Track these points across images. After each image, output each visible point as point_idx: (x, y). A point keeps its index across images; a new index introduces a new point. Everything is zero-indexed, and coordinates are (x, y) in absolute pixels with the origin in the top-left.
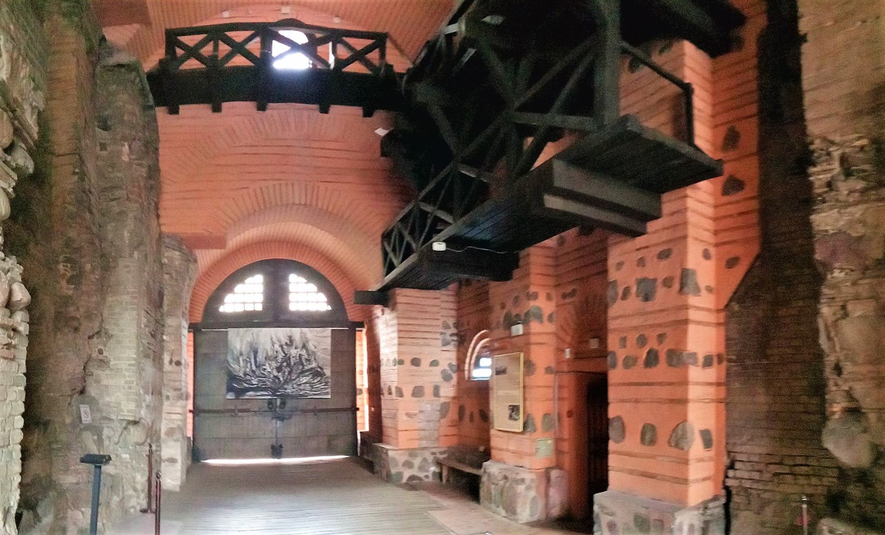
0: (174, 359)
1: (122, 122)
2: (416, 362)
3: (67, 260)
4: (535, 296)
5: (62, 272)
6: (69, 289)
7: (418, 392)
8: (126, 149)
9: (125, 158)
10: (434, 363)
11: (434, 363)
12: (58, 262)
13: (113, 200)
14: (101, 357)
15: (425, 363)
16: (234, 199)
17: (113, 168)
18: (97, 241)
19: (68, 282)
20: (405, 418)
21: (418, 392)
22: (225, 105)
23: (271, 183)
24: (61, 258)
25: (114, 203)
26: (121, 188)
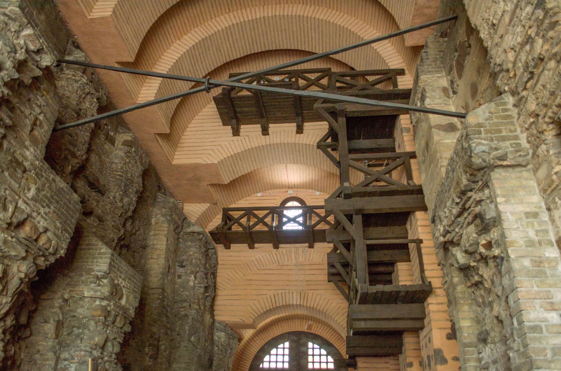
1: (191, 263)
5: (147, 352)
6: (149, 361)
9: (191, 284)
12: (145, 347)
13: (182, 308)
17: (184, 289)
18: (169, 332)
19: (150, 358)
23: (280, 292)
24: (147, 344)
25: (182, 309)
26: (185, 301)
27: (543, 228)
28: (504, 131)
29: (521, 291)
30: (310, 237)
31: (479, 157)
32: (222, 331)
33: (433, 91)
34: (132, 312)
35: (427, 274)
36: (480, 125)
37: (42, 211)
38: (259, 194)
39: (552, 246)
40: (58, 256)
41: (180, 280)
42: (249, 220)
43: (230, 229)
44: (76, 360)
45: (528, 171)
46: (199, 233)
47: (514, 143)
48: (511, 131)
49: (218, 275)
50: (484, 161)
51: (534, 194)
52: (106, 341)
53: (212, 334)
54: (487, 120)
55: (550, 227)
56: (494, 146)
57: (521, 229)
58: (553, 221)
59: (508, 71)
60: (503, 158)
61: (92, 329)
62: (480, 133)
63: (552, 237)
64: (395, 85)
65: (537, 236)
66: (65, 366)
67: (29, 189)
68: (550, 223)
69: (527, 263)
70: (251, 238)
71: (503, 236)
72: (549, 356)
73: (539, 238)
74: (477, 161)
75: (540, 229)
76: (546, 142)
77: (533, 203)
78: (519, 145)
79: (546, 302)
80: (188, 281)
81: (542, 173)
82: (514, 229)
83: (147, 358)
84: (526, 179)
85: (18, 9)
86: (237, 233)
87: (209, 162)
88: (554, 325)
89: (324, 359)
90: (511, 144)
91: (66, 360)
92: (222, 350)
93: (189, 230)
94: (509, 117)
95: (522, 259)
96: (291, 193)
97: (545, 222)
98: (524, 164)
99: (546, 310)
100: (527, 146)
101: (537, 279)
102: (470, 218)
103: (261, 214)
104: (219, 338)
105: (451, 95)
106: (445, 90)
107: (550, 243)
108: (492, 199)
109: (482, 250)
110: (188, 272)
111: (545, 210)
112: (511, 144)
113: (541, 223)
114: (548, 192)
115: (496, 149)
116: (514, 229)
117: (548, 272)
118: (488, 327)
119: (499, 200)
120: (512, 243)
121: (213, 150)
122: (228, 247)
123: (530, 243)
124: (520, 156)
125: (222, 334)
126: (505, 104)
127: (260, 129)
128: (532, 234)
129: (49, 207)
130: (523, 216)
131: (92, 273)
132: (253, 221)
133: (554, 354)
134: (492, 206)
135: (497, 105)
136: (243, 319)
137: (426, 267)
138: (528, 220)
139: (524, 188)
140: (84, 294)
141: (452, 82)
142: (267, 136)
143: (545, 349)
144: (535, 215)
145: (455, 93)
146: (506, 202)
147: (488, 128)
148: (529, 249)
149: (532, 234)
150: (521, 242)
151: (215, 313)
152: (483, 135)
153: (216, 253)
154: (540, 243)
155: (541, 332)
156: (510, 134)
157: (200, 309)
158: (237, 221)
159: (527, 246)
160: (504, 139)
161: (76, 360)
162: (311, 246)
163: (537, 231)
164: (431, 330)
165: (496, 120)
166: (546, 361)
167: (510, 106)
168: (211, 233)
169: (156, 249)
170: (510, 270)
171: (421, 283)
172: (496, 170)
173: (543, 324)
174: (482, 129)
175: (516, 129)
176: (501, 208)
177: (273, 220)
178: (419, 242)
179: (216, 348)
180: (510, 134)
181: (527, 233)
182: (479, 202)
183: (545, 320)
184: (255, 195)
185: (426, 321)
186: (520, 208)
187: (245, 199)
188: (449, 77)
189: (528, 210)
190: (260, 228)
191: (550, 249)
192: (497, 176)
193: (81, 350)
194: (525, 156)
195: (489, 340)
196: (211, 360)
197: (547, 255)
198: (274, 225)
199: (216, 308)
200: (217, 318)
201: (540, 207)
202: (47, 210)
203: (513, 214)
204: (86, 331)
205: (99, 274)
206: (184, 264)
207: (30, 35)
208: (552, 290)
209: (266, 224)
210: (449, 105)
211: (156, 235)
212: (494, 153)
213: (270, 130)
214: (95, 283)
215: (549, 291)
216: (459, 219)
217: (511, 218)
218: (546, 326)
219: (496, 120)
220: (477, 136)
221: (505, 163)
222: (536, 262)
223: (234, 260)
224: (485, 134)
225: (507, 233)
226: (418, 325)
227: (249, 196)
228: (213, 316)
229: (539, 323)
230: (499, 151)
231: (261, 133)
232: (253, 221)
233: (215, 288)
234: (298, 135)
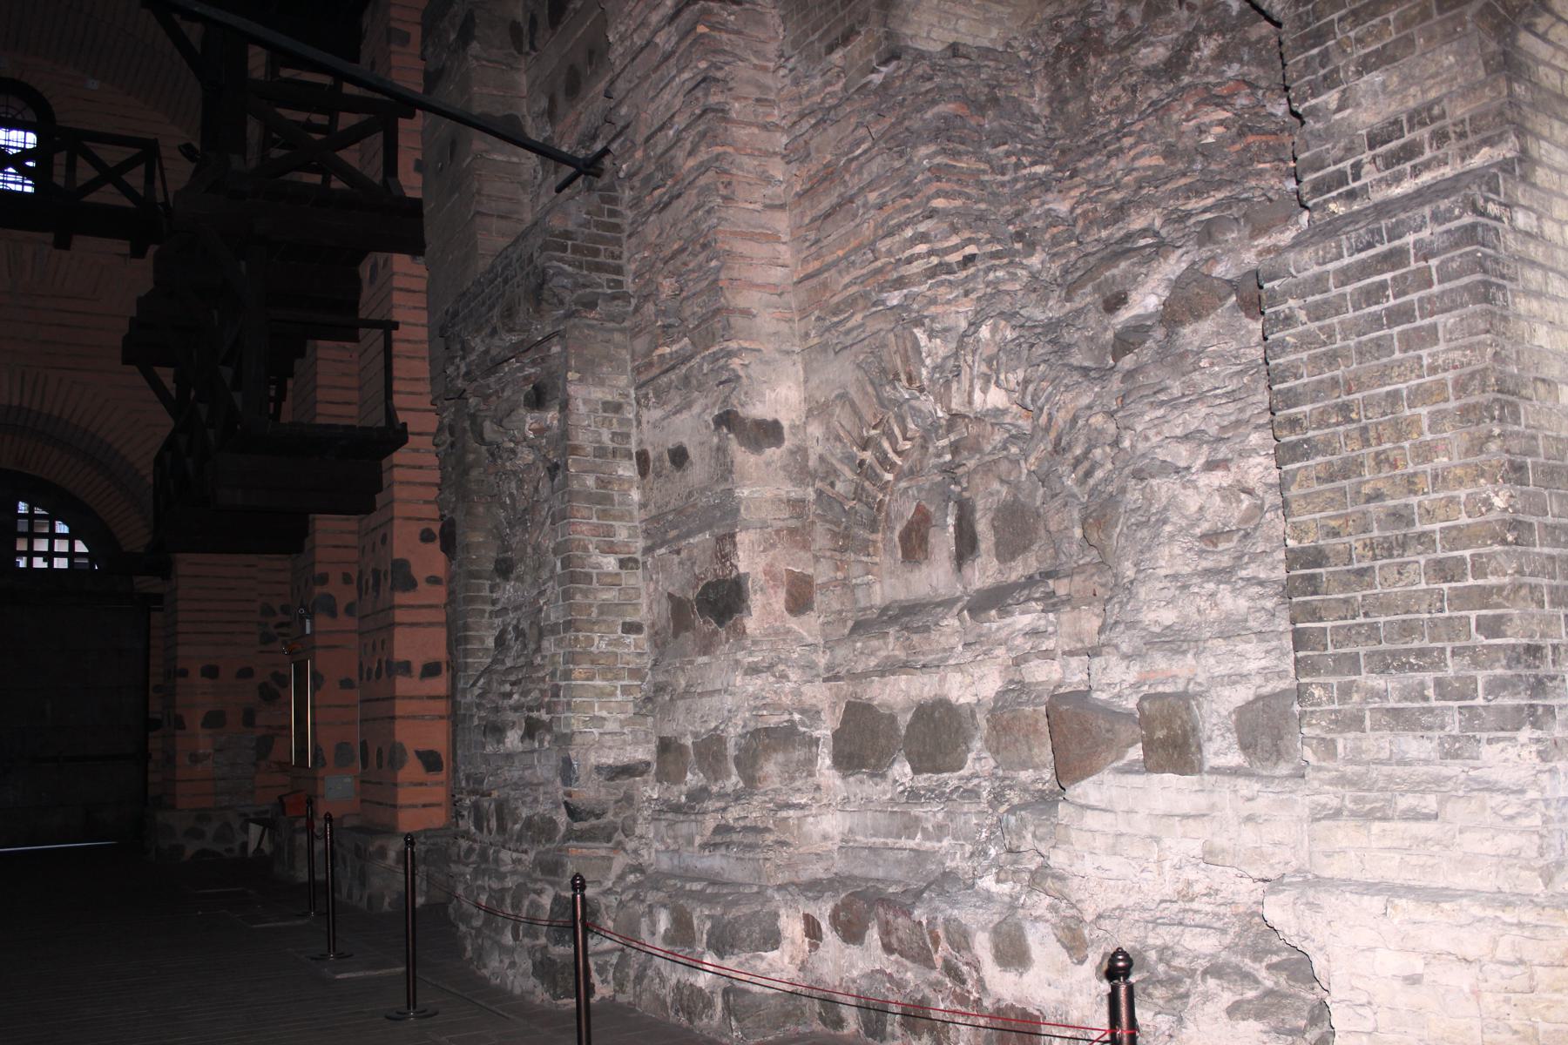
2: (211, 672)
4: (324, 579)
7: (214, 720)
10: (246, 673)
11: (246, 673)
27: (625, 430)
35: (398, 400)
36: (567, 235)
51: (624, 372)
56: (581, 280)
69: (590, 481)
78: (619, 284)
84: (617, 346)
88: (609, 574)
89: (61, 546)
90: (609, 281)
95: (585, 476)
105: (527, 48)
113: (624, 422)
115: (584, 286)
117: (616, 498)
123: (601, 452)
133: (601, 613)
137: (397, 386)
139: (610, 359)
143: (591, 605)
144: (617, 408)
146: (580, 380)
150: (589, 449)
152: (569, 255)
154: (614, 453)
160: (599, 268)
163: (614, 434)
164: (392, 519)
166: (589, 621)
171: (382, 424)
176: (571, 389)
183: (599, 566)
185: (380, 499)
186: (598, 394)
189: (609, 398)
191: (626, 463)
201: (627, 396)
203: (585, 402)
208: (616, 524)
217: (582, 409)
219: (594, 230)
224: (574, 252)
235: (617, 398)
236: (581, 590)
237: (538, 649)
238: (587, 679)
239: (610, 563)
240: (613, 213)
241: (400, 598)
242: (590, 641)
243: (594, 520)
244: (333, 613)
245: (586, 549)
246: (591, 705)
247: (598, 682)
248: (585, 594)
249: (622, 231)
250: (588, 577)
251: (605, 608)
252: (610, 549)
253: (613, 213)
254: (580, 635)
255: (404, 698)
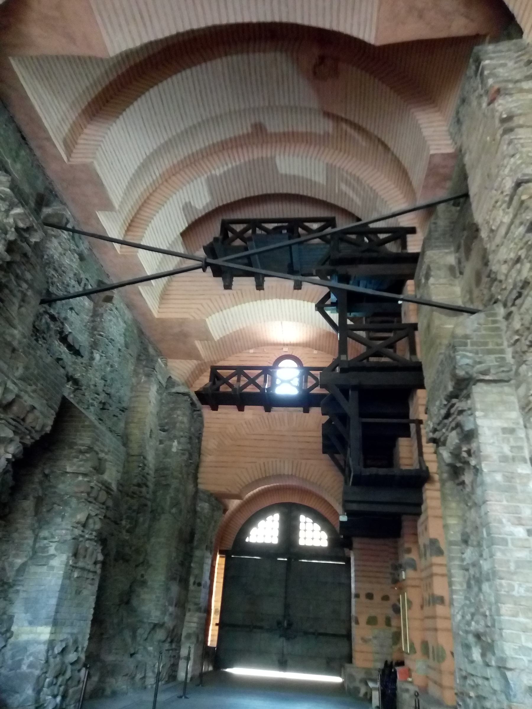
0: (197, 581)
2: (370, 596)
3: (128, 518)
8: (175, 443)
9: (174, 450)
10: (386, 598)
14: (142, 579)
15: (377, 598)
16: (247, 469)
20: (360, 642)
21: (372, 621)
22: (246, 407)
27: (519, 444)
28: (490, 343)
29: (490, 505)
30: (306, 401)
31: (463, 370)
32: (206, 502)
33: (439, 269)
34: (114, 486)
35: (426, 457)
36: (466, 337)
37: (29, 389)
38: (251, 351)
39: (526, 462)
40: (43, 433)
41: (162, 446)
42: (239, 380)
43: (218, 389)
44: (56, 539)
45: (510, 386)
46: (184, 394)
47: (500, 358)
48: (498, 345)
49: (203, 438)
50: (467, 373)
51: (514, 410)
52: (88, 518)
53: (194, 505)
54: (475, 331)
55: (525, 445)
56: (478, 360)
57: (497, 444)
58: (528, 438)
59: (501, 281)
60: (485, 372)
61: (73, 506)
62: (466, 345)
63: (527, 454)
64: (404, 245)
65: (511, 452)
66: (44, 545)
67: (17, 368)
68: (525, 440)
69: (499, 477)
70: (240, 400)
71: (479, 449)
72: (512, 567)
73: (514, 454)
74: (461, 373)
75: (515, 445)
76: (527, 363)
77: (511, 419)
78: (503, 359)
79: (515, 517)
80: (171, 446)
81: (522, 390)
82: (490, 444)
83: (124, 532)
84: (508, 394)
85: (8, 190)
86: (225, 394)
87: (197, 318)
88: (520, 539)
90: (496, 358)
91: (45, 538)
92: (204, 523)
93: (174, 390)
94: (498, 329)
96: (286, 351)
97: (521, 438)
98: (506, 379)
99: (513, 524)
100: (512, 361)
101: (506, 494)
102: (453, 424)
103: (252, 373)
104: (203, 508)
105: (458, 274)
106: (451, 269)
107: (524, 460)
108: (471, 411)
109: (464, 455)
110: (172, 436)
111: (522, 427)
112: (496, 358)
114: (527, 410)
115: (480, 363)
116: (490, 444)
117: (519, 488)
118: (468, 530)
119: (477, 414)
120: (487, 457)
121: (202, 304)
122: (215, 408)
123: (504, 459)
124: (503, 371)
125: (206, 505)
126: (494, 315)
127: (254, 283)
128: (506, 450)
129: (37, 386)
130: (500, 431)
131: (75, 447)
132: (244, 381)
133: (518, 567)
134: (471, 418)
135: (487, 316)
136: (229, 489)
138: (505, 436)
140: (66, 469)
141: (459, 262)
142: (262, 291)
143: (508, 561)
144: (512, 431)
145: (461, 273)
146: (485, 416)
147: (475, 340)
148: (503, 464)
149: (506, 450)
150: (495, 457)
151: (199, 481)
152: (469, 347)
153: (201, 416)
154: (514, 459)
155: (507, 545)
156: (496, 347)
157: (183, 477)
158: (226, 381)
159: (500, 462)
160: (490, 352)
161: (56, 539)
162: (306, 411)
163: (512, 447)
165: (484, 332)
166: (509, 572)
167: (500, 318)
168: (198, 393)
169: (138, 412)
170: (482, 483)
172: (480, 384)
173: (509, 538)
174: (469, 341)
175: (503, 342)
176: (479, 422)
177: (265, 381)
178: (420, 422)
179: (198, 520)
180: (496, 347)
181: (502, 448)
182: (461, 412)
183: (511, 534)
184: (247, 351)
185: (423, 507)
186: (498, 424)
187: (236, 355)
188: (457, 255)
189: (506, 425)
190: (251, 389)
191: (524, 466)
192: (478, 390)
193: (62, 529)
194: (508, 371)
195: (470, 543)
196: (192, 534)
197: (519, 471)
198: (266, 387)
199: (199, 475)
200: (200, 487)
201: (518, 424)
202: (34, 387)
203: (490, 428)
204: (68, 509)
205: (82, 448)
206: (166, 428)
207: (19, 214)
208: (521, 505)
209: (258, 386)
210: (455, 285)
211: (137, 396)
212: (478, 366)
213: (266, 285)
214: (78, 458)
215: (518, 506)
216: (446, 421)
218: (512, 539)
220: (462, 348)
221: (487, 378)
222: (507, 477)
223: (221, 421)
225: (483, 447)
226: (416, 508)
227: (240, 352)
228: (196, 484)
229: (505, 536)
230: (483, 365)
231: (254, 287)
232: (244, 381)
233: (200, 454)
234: (296, 291)
235: (512, 425)
236: (500, 550)
237: (480, 589)
238: (513, 616)
239: (520, 532)
240: (494, 322)
241: (436, 560)
242: (512, 588)
243: (505, 503)
244: (415, 569)
245: (500, 522)
246: (519, 637)
247: (522, 619)
248: (504, 552)
249: (501, 330)
250: (505, 542)
251: (520, 564)
252: (519, 522)
253: (494, 322)
254: (503, 582)
255: (441, 618)
